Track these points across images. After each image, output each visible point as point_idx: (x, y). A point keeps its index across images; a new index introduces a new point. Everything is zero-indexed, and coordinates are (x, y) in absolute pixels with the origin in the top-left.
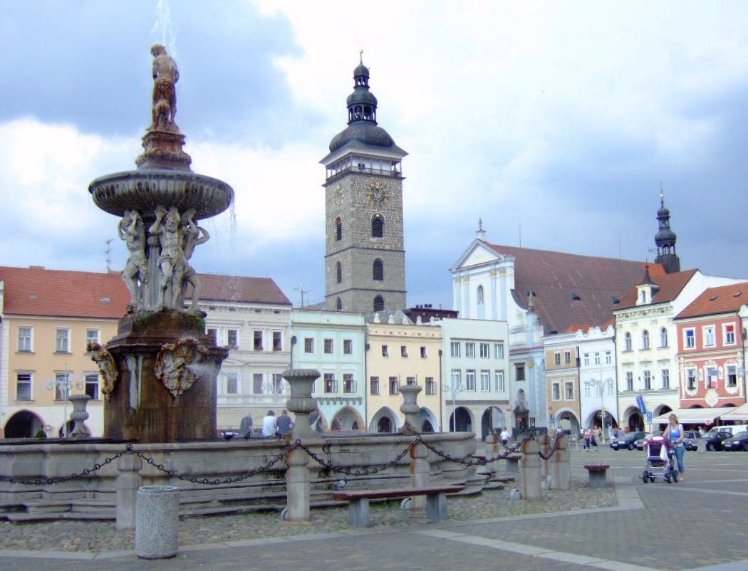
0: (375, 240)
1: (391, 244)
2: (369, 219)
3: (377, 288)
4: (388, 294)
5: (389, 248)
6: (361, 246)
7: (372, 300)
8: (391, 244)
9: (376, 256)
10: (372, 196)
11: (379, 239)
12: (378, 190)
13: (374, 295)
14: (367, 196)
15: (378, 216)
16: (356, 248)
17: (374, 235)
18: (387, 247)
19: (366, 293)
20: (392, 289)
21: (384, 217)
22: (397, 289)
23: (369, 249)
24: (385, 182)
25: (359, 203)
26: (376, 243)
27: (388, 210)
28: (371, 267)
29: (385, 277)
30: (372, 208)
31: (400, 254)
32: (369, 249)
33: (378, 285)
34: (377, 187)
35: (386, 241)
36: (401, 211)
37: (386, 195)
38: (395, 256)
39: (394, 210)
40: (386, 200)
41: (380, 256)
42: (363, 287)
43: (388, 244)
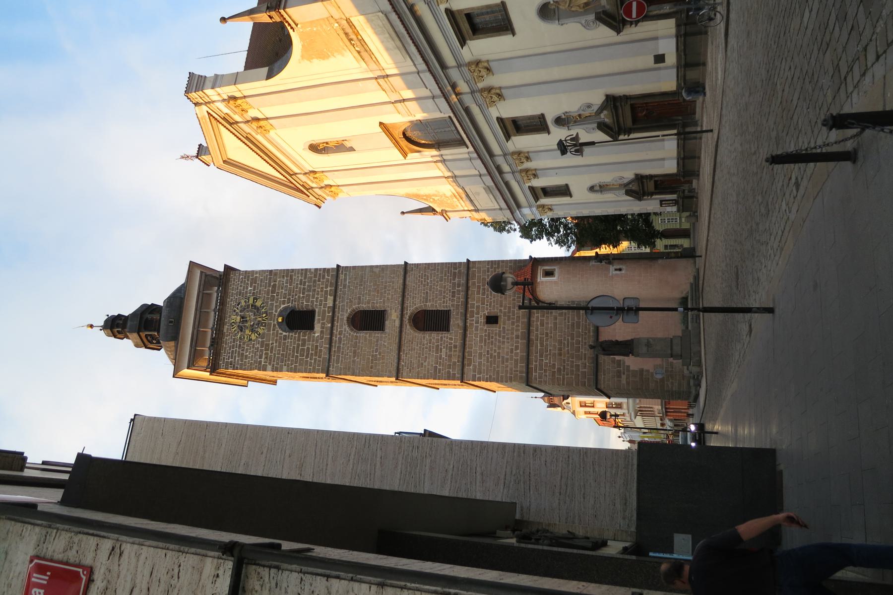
0: (317, 327)
1: (326, 292)
2: (285, 338)
3: (397, 323)
4: (408, 303)
5: (332, 298)
6: (327, 356)
7: (419, 335)
9: (343, 327)
11: (317, 318)
12: (242, 317)
13: (408, 329)
14: (250, 340)
15: (280, 320)
16: (329, 367)
17: (311, 328)
19: (404, 348)
20: (400, 290)
21: (283, 306)
22: (401, 281)
23: (331, 339)
24: (231, 302)
25: (261, 357)
26: (322, 328)
27: (273, 299)
28: (362, 334)
29: (379, 306)
30: (269, 331)
31: (342, 277)
32: (331, 339)
33: (393, 319)
35: (321, 304)
36: (276, 274)
38: (345, 286)
40: (258, 304)
41: (343, 315)
42: (394, 354)
43: (326, 299)
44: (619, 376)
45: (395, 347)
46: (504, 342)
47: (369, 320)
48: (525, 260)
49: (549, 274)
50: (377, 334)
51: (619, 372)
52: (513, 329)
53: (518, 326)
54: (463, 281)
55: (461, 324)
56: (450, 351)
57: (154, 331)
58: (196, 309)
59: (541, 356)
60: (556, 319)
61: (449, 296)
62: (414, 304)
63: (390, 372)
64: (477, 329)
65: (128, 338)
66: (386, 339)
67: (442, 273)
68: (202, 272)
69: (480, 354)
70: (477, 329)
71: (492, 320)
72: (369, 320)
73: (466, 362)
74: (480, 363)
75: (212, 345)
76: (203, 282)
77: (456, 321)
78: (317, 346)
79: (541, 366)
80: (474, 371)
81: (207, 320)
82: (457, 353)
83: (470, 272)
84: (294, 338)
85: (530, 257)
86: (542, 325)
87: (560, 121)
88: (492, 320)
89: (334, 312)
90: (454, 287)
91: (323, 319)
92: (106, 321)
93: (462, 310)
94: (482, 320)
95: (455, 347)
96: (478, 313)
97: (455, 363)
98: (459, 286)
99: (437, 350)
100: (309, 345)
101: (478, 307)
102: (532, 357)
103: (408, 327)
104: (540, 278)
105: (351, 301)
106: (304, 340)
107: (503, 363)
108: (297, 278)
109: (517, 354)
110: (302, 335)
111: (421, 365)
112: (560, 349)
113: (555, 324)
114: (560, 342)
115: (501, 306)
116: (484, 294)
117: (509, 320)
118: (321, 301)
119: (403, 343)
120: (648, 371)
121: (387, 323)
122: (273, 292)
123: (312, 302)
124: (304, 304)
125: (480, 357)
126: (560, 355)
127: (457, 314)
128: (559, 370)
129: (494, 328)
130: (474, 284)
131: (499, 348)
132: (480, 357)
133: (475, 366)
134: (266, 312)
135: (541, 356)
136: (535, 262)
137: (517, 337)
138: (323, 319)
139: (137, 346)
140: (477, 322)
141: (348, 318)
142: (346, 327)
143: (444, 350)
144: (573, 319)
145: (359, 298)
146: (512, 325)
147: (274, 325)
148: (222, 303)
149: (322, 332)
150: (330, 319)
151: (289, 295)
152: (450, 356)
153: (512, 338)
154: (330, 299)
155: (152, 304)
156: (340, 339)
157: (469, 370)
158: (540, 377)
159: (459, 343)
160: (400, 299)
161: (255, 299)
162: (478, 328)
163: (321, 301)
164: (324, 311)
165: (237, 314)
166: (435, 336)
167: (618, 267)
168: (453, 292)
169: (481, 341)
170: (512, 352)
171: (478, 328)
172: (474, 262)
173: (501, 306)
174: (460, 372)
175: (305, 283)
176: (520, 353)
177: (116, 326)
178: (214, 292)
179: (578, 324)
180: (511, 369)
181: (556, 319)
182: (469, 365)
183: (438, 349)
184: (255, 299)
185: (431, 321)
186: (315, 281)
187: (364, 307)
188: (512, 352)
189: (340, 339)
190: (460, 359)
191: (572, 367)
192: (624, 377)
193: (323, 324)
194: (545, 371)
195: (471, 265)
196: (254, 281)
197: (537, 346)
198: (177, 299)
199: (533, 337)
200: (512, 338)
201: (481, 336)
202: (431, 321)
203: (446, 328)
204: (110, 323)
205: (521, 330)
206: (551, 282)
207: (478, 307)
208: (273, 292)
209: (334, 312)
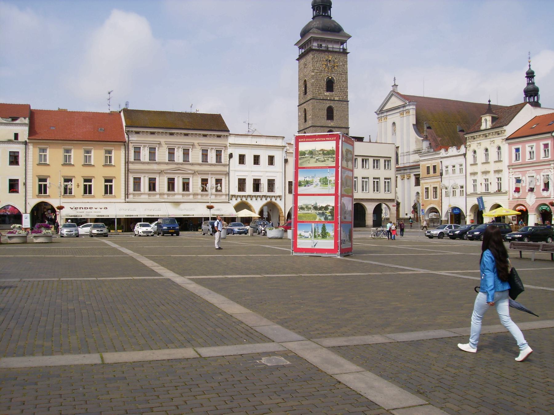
3: (330, 125)
9: (328, 104)
10: (326, 65)
12: (330, 60)
17: (327, 91)
18: (337, 98)
19: (322, 128)
26: (328, 96)
27: (338, 74)
28: (325, 112)
29: (335, 118)
31: (345, 103)
34: (330, 59)
35: (336, 95)
40: (336, 68)
41: (332, 104)
42: (319, 124)
45: (322, 125)
84: (324, 84)
108: (344, 84)
124: (335, 87)
161: (337, 66)
184: (337, 66)
187: (335, 112)
196: (344, 65)
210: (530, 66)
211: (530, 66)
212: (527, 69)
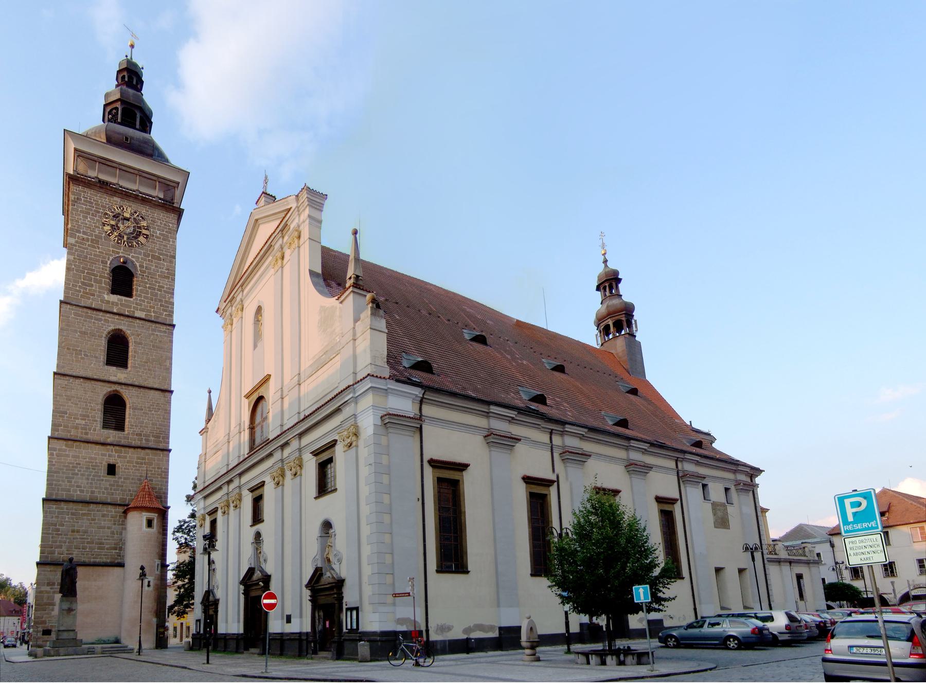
0: (115, 298)
1: (149, 311)
3: (113, 379)
4: (134, 391)
5: (143, 316)
8: (149, 311)
9: (113, 324)
11: (124, 298)
13: (107, 389)
17: (114, 291)
18: (138, 314)
19: (89, 384)
21: (138, 264)
24: (144, 210)
26: (113, 303)
28: (103, 344)
37: (144, 231)
39: (159, 259)
40: (141, 239)
41: (124, 326)
44: (48, 584)
45: (89, 375)
46: (88, 479)
47: (118, 350)
48: (166, 502)
49: (150, 523)
50: (103, 357)
51: (54, 584)
52: (101, 488)
53: (103, 493)
54: (151, 445)
55: (109, 441)
56: (82, 429)
57: (122, 119)
58: (139, 170)
59: (73, 514)
60: (109, 528)
61: (138, 430)
62: (129, 396)
63: (63, 367)
64: (102, 455)
65: (117, 86)
66: (97, 366)
67: (160, 425)
68: (178, 183)
69: (78, 457)
70: (102, 455)
71: (111, 470)
72: (118, 350)
73: (70, 442)
74: (68, 456)
75: (100, 181)
76: (168, 183)
77: (112, 435)
78: (93, 295)
79: (62, 513)
80: (60, 450)
81: (129, 180)
82: (79, 435)
83: (158, 452)
85: (169, 508)
86: (103, 516)
87: (258, 535)
88: (111, 470)
89: (128, 316)
90: (145, 435)
91: (122, 305)
92: (135, 65)
93: (123, 442)
94: (112, 461)
95: (86, 434)
96: (119, 457)
97: (69, 432)
98: (147, 440)
99: (84, 416)
100: (95, 287)
101: (125, 457)
102: (71, 505)
103: (109, 390)
104: (146, 515)
105: (138, 335)
106: (100, 282)
107: (67, 478)
109: (75, 491)
110: (106, 282)
111: (69, 398)
112: (78, 531)
113: (104, 528)
114: (86, 532)
115: (125, 479)
116: (137, 463)
117: (110, 485)
118: (141, 305)
119: (93, 382)
120: (53, 610)
121: (114, 368)
122: (153, 256)
123: (140, 296)
124: (137, 287)
125: (73, 456)
126: (73, 531)
127: (119, 437)
128: (58, 530)
129: (103, 470)
130: (148, 454)
131: (82, 475)
132: (73, 456)
133: (65, 451)
134: (132, 246)
135: (73, 514)
136: (163, 513)
137: (93, 492)
138: (122, 305)
139: (107, 95)
140: (110, 456)
141: (121, 330)
142: (112, 327)
143: (83, 422)
144: (107, 544)
145: (140, 343)
146: (104, 488)
147: (118, 253)
148: (145, 200)
149: (108, 302)
150: (122, 312)
151: (149, 273)
152: (77, 428)
153: (91, 487)
154: (142, 315)
155: (151, 123)
156: (101, 320)
157: (61, 445)
158: (50, 512)
159: (90, 437)
160: (136, 383)
161: (147, 237)
162: (103, 456)
163: (141, 305)
164: (130, 307)
165: (132, 214)
166: (99, 416)
167: (151, 584)
168: (140, 435)
169: (91, 458)
170: (78, 486)
171: (103, 456)
172: (168, 456)
173: (125, 479)
174: (60, 436)
175: (160, 291)
176: (77, 494)
177: (131, 76)
178: (157, 193)
179: (102, 548)
180: (60, 485)
181: (109, 528)
182: (66, 446)
183: (84, 417)
184: (147, 237)
185: (114, 410)
186: (161, 301)
188: (78, 486)
189: (101, 320)
190: (72, 438)
191: (60, 542)
192: (48, 588)
193: (117, 304)
194: (57, 517)
195: (165, 453)
197: (82, 509)
198: (151, 152)
199: (92, 506)
200: (91, 487)
201: (96, 459)
202: (114, 410)
203: (106, 426)
204: (133, 69)
205: (100, 496)
206: (141, 525)
207: (125, 457)
208: (153, 256)
209: (128, 316)
210: (605, 261)
211: (605, 261)
212: (600, 268)
